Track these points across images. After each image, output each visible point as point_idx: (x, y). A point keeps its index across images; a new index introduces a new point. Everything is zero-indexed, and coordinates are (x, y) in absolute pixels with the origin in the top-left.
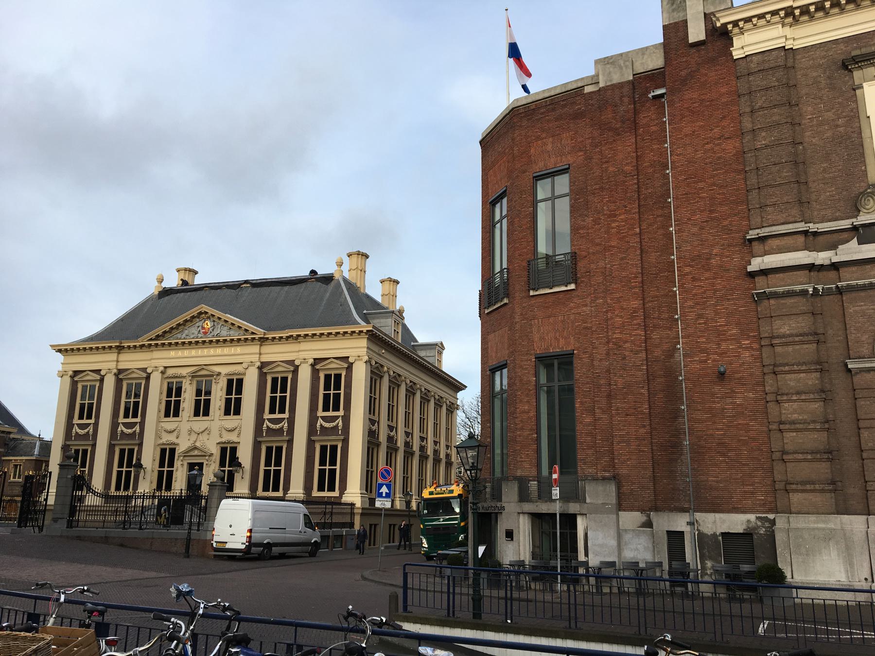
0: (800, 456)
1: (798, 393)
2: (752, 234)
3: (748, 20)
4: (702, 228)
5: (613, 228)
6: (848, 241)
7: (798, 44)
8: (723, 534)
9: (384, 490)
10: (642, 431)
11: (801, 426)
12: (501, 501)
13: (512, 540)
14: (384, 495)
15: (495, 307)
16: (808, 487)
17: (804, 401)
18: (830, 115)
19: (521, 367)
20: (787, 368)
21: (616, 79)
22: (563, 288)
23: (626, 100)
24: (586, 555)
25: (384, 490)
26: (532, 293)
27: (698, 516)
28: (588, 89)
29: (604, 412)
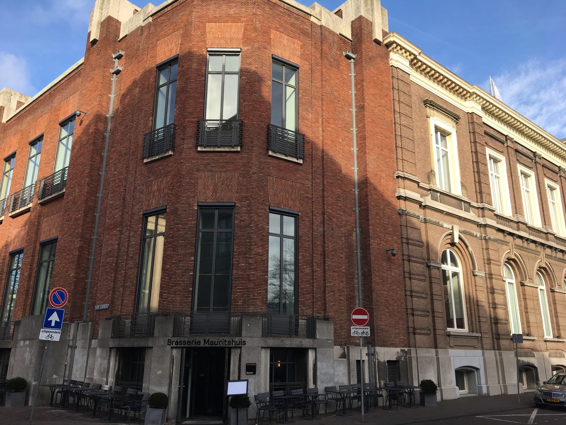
0: (420, 313)
1: (418, 275)
2: (401, 174)
3: (402, 48)
4: (378, 158)
5: (328, 131)
6: (427, 196)
7: (412, 78)
8: (388, 361)
9: (54, 318)
10: (342, 285)
11: (419, 295)
12: (240, 335)
13: (255, 373)
14: (53, 324)
15: (217, 149)
16: (423, 332)
17: (420, 280)
18: (419, 124)
19: (257, 213)
20: (414, 259)
21: (331, 27)
22: (295, 160)
23: (335, 45)
24: (315, 382)
25: (54, 318)
26: (270, 153)
27: (378, 349)
28: (312, 19)
29: (318, 266)
